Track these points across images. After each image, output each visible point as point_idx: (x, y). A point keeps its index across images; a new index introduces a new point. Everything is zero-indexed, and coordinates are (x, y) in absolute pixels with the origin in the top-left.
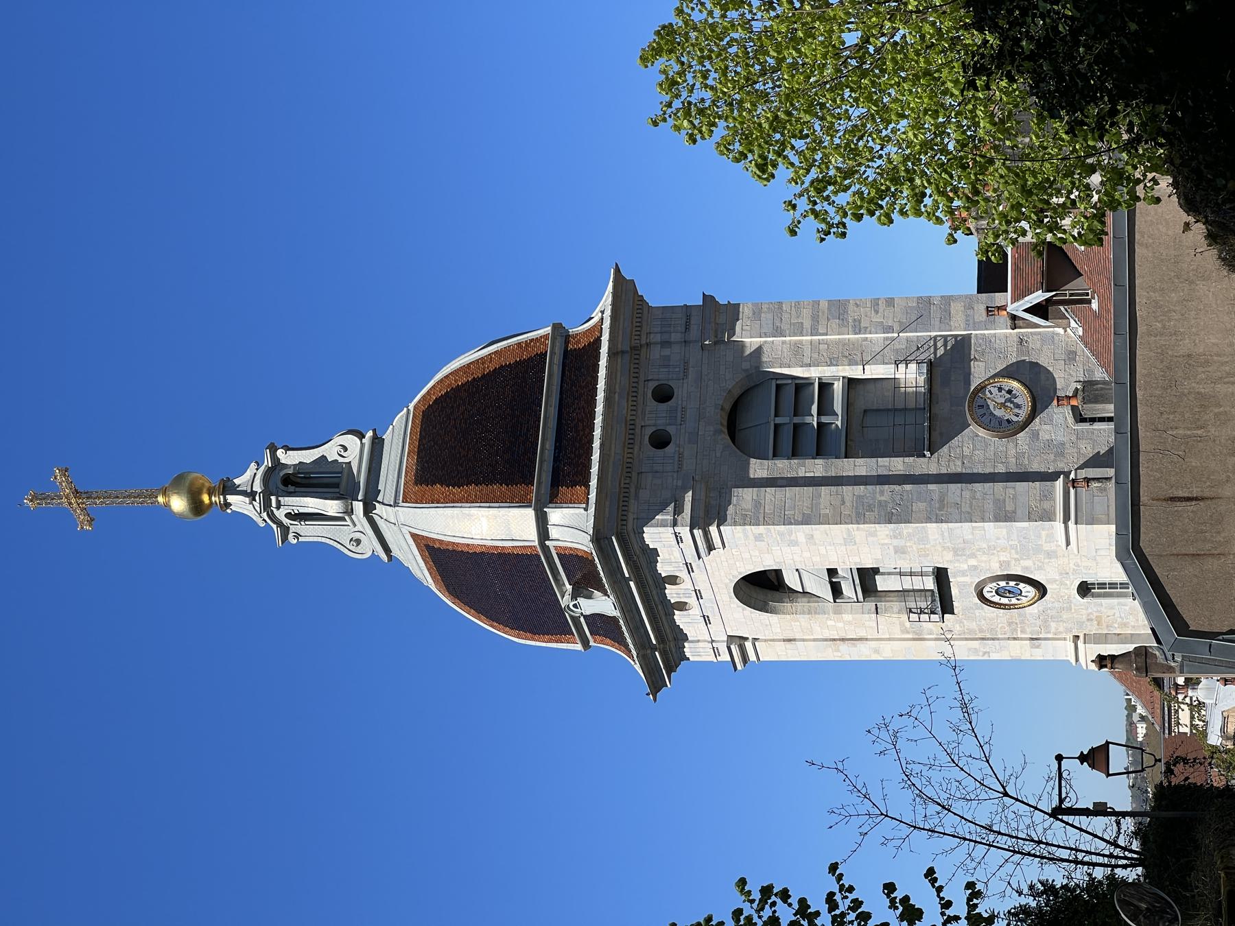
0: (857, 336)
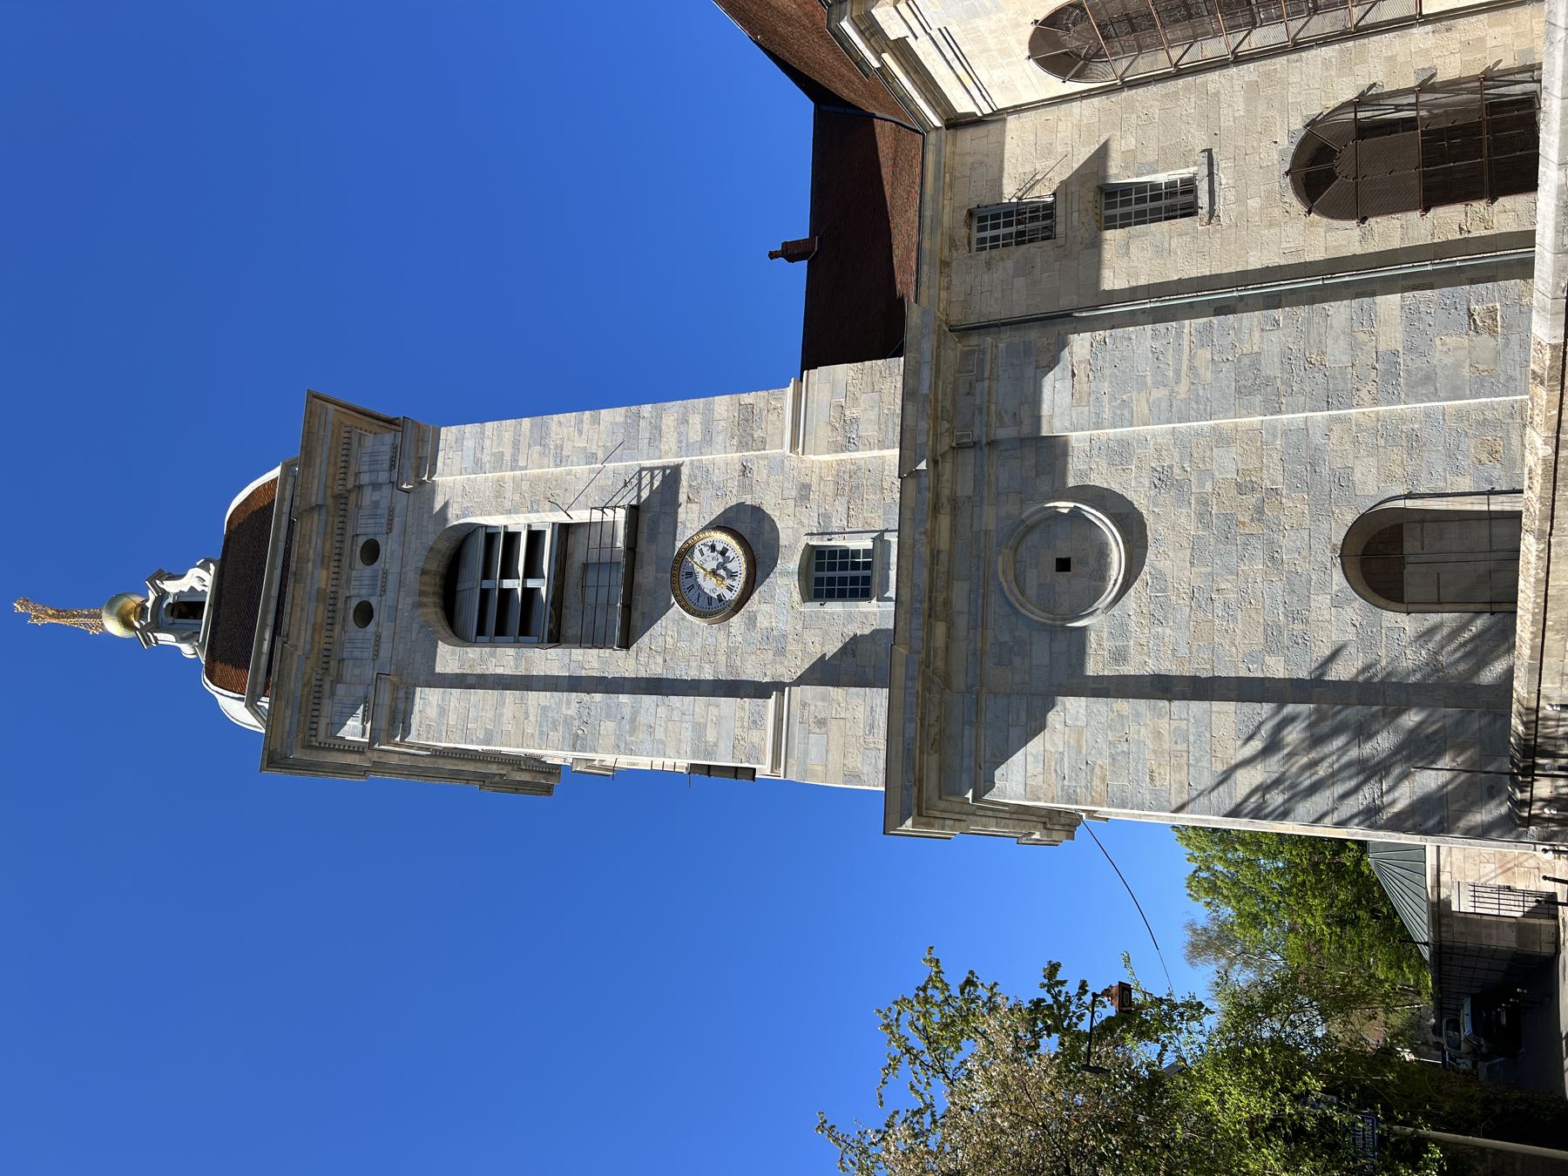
0: (559, 469)
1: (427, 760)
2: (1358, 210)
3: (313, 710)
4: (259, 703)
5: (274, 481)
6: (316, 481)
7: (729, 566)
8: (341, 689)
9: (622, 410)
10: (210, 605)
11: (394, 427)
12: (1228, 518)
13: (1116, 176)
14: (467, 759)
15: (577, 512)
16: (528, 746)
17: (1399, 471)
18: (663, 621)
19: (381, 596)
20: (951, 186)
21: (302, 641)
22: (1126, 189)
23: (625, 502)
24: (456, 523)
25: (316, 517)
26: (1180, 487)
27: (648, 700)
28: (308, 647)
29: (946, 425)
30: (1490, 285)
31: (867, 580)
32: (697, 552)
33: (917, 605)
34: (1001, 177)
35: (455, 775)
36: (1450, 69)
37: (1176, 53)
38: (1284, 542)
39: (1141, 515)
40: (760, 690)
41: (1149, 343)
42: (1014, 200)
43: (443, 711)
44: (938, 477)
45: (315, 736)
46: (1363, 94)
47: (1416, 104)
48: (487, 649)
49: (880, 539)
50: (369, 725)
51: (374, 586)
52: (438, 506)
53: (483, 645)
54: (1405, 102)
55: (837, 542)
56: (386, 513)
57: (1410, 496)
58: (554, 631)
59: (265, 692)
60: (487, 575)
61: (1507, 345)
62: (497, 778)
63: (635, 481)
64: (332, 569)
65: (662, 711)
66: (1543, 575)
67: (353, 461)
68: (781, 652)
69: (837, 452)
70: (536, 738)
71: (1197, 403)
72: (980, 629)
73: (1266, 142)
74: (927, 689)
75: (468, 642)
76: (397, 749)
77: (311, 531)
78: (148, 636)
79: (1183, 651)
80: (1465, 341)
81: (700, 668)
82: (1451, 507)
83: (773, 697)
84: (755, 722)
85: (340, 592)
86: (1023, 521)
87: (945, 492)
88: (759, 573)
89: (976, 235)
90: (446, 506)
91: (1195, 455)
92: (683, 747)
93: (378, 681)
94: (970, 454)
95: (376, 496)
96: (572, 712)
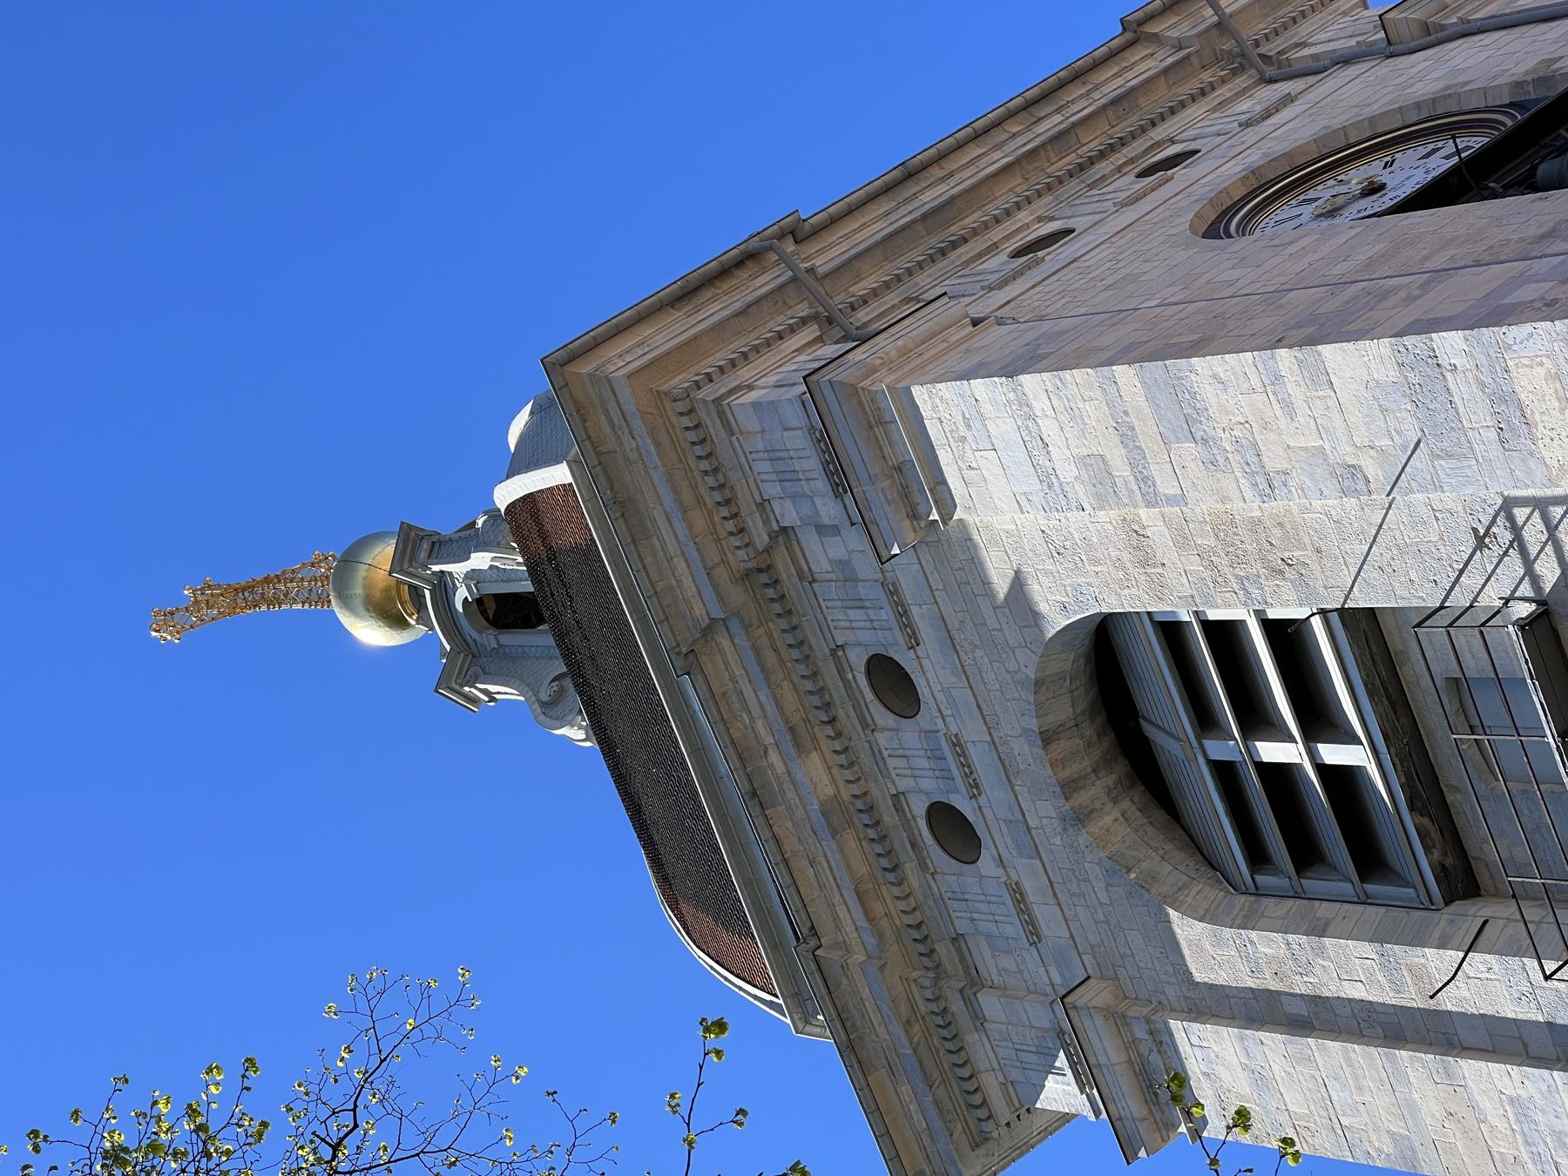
8: (989, 1003)
21: (849, 928)
25: (725, 643)
52: (1001, 586)
64: (826, 745)
67: (734, 477)
77: (733, 679)
90: (1018, 582)
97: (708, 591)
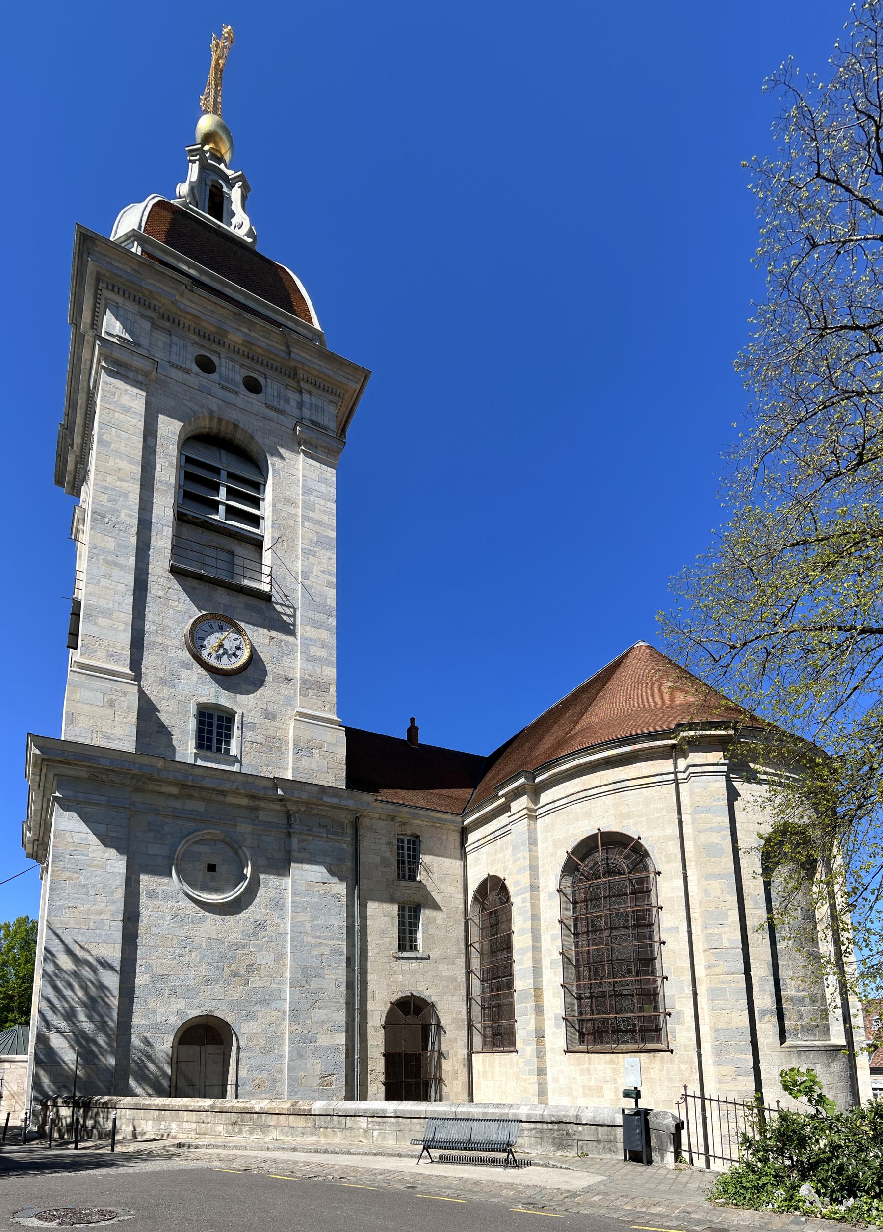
1: (85, 383)
2: (389, 1025)
3: (129, 294)
4: (136, 243)
5: (311, 321)
6: (308, 357)
7: (225, 657)
9: (334, 605)
10: (220, 226)
11: (340, 432)
12: (234, 959)
13: (424, 914)
14: (86, 420)
15: (270, 556)
16: (96, 475)
17: (253, 1043)
18: (188, 601)
19: (219, 384)
20: (433, 826)
22: (417, 918)
23: (274, 593)
24: (269, 462)
26: (254, 935)
27: (130, 579)
28: (182, 306)
29: (303, 809)
30: (344, 1083)
31: (209, 748)
32: (236, 636)
33: (191, 778)
34: (433, 855)
35: (72, 405)
36: (446, 1065)
37: (477, 945)
38: (217, 987)
39: (239, 913)
40: (136, 663)
41: (336, 924)
42: (421, 861)
43: (126, 410)
44: (272, 801)
45: (107, 287)
46: (442, 1028)
47: (433, 1051)
48: (175, 461)
49: (235, 760)
50: (115, 340)
51: (227, 380)
53: (179, 460)
54: (435, 1046)
55: (236, 733)
56: (280, 407)
57: (238, 1048)
58: (185, 518)
59: (146, 253)
60: (231, 476)
61: (313, 1091)
62: (69, 441)
63: (287, 603)
65: (121, 588)
66: (191, 1109)
68: (163, 682)
69: (294, 741)
70: (103, 483)
71: (301, 946)
72: (173, 814)
73: (428, 984)
74: (133, 777)
75: (182, 447)
76: (95, 361)
78: (196, 155)
79: (154, 930)
80: (318, 1073)
81: (154, 622)
82: (230, 1067)
83: (131, 672)
84: (112, 656)
85: (223, 350)
86: (240, 847)
87: (262, 804)
88: (219, 677)
89: (406, 838)
91: (272, 944)
92: (94, 599)
93: (152, 361)
94: (285, 822)
95: (293, 404)
96: (123, 517)
97: (298, 358)
